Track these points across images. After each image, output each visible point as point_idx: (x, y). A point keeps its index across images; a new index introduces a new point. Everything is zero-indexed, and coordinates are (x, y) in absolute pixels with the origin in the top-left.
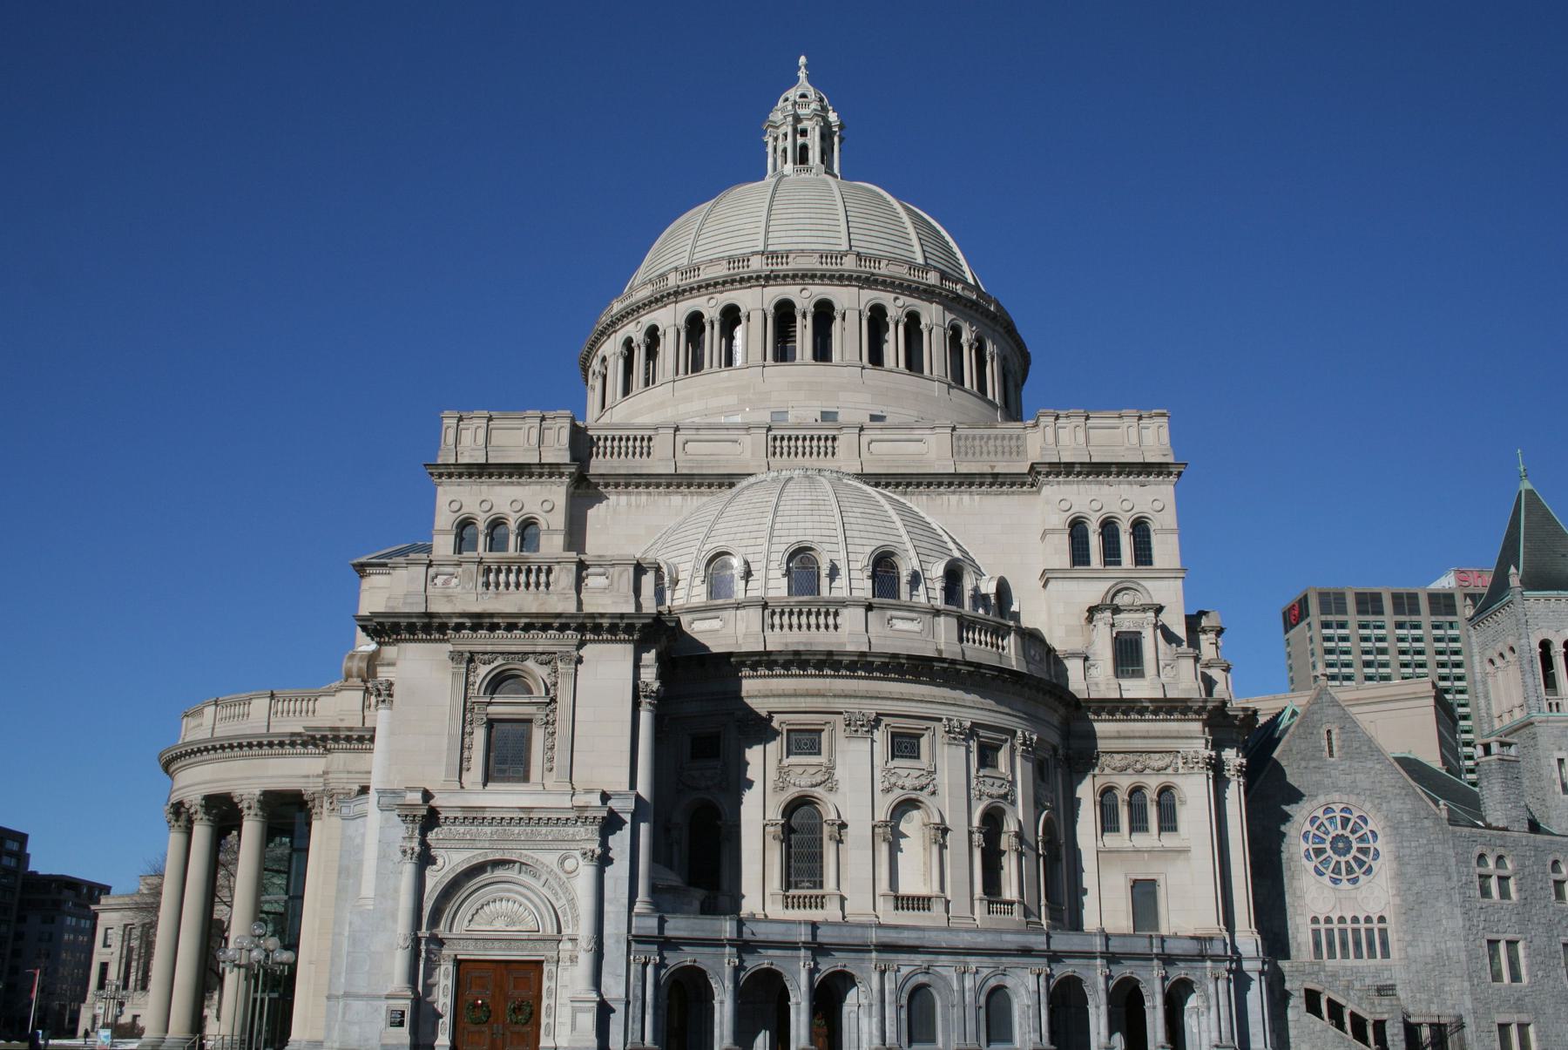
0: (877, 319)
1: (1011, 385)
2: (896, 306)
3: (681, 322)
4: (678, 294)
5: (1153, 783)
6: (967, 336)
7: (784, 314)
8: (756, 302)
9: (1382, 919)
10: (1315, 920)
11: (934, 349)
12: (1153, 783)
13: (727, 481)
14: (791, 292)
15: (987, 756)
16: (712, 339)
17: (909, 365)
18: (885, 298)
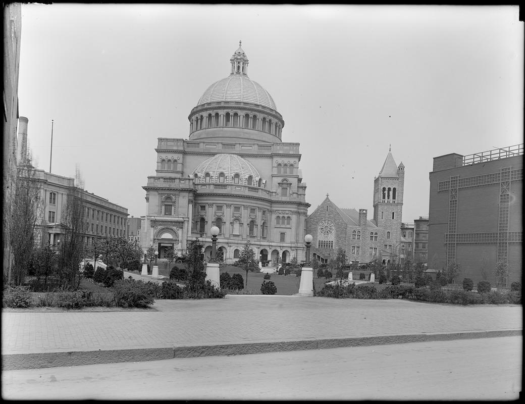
0: (247, 116)
1: (278, 128)
2: (251, 116)
3: (207, 116)
4: (206, 109)
5: (286, 216)
6: (267, 120)
7: (228, 115)
8: (222, 113)
9: (332, 242)
10: (320, 241)
11: (259, 123)
12: (286, 216)
13: (214, 154)
14: (229, 111)
15: (253, 210)
16: (213, 119)
17: (253, 127)
18: (249, 112)
